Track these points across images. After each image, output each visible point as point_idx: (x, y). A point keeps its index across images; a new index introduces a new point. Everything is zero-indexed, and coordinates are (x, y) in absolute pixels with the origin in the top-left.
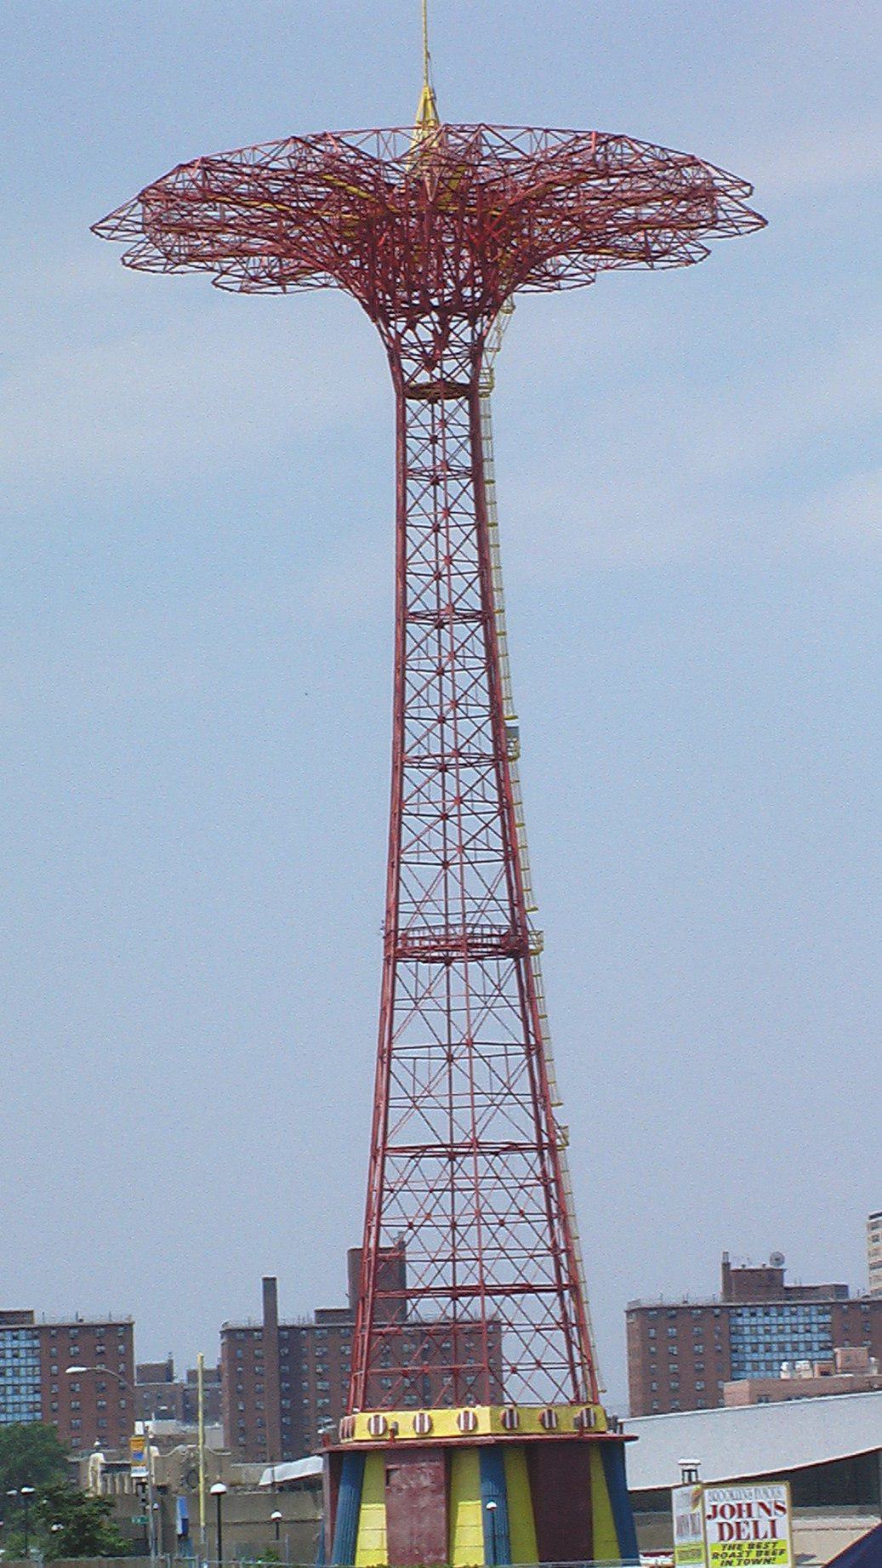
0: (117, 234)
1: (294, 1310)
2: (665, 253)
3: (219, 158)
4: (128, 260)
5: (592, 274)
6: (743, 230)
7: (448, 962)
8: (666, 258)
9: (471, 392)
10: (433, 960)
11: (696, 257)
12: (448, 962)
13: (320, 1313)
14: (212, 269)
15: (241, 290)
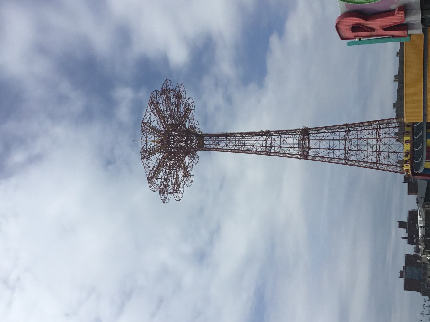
0: (167, 198)
1: (406, 235)
2: (190, 105)
3: (147, 176)
4: (177, 199)
5: (195, 122)
6: (183, 89)
7: (309, 148)
8: (191, 106)
9: (202, 137)
10: (308, 151)
11: (192, 101)
12: (309, 148)
13: (406, 232)
14: (183, 186)
15: (192, 183)
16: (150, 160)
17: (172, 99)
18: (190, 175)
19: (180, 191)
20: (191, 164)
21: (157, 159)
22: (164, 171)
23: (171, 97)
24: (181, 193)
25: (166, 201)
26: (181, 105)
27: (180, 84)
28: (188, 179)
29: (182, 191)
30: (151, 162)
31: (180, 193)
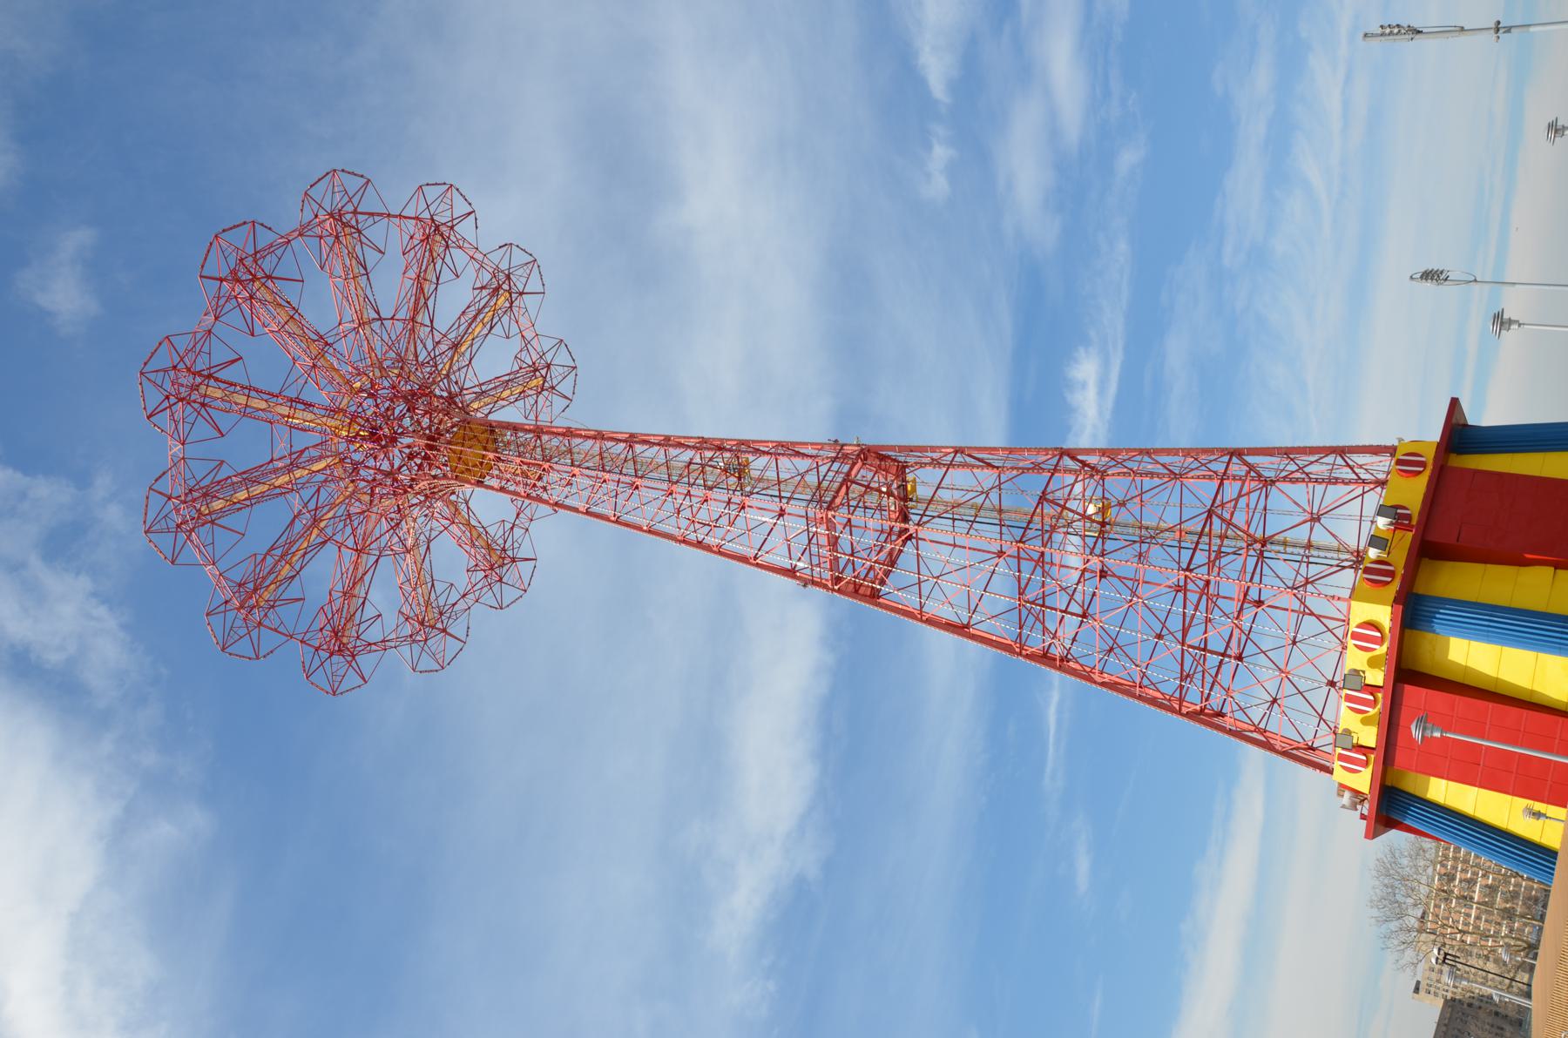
14: (385, 649)
16: (199, 413)
17: (446, 275)
18: (444, 630)
19: (353, 656)
20: (471, 596)
21: (272, 461)
22: (295, 532)
23: (448, 259)
24: (354, 664)
25: (244, 647)
26: (498, 329)
27: (519, 258)
28: (426, 640)
29: (366, 661)
30: (203, 429)
31: (350, 663)
